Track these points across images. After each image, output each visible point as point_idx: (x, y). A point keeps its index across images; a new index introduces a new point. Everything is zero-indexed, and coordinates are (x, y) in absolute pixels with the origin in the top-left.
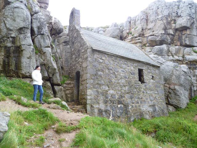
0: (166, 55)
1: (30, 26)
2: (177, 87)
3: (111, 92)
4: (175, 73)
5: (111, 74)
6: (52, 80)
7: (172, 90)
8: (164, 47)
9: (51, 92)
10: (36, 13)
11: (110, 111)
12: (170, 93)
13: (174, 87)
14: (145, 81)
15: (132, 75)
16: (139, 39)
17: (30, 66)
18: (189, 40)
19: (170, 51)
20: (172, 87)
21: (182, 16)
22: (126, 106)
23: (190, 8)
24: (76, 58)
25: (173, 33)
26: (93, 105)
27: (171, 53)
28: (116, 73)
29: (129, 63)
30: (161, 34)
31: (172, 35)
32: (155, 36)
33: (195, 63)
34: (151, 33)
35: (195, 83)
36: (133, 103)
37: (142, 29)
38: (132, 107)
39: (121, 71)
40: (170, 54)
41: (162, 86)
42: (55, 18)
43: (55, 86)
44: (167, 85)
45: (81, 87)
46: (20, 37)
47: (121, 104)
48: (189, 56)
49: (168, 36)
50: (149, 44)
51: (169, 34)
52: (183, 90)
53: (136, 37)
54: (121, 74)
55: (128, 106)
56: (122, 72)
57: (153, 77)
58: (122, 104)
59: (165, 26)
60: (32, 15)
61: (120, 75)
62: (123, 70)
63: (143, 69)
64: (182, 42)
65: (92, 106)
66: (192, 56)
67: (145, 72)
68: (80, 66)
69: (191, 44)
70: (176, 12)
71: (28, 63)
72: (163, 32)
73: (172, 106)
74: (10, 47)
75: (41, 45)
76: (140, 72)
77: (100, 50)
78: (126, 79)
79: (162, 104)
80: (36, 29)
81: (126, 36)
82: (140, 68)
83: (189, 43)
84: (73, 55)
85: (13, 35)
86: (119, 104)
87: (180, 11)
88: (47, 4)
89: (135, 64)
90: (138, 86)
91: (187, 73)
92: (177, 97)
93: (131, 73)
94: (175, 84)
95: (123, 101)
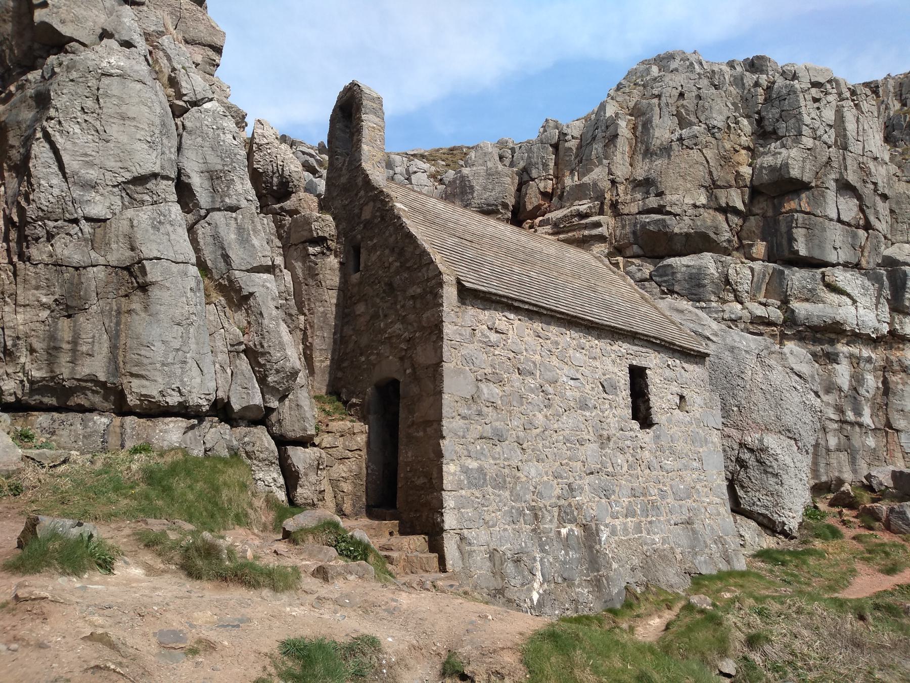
0: (713, 298)
2: (772, 441)
3: (532, 470)
4: (759, 377)
5: (532, 391)
6: (279, 421)
7: (751, 450)
8: (708, 261)
9: (275, 475)
10: (196, 103)
11: (534, 559)
12: (741, 467)
13: (761, 441)
14: (656, 418)
15: (605, 396)
16: (598, 225)
17: (185, 362)
18: (809, 239)
19: (730, 284)
21: (781, 132)
22: (590, 534)
23: (816, 100)
24: (375, 316)
25: (740, 206)
26: (465, 532)
27: (735, 291)
28: (550, 390)
30: (695, 206)
31: (735, 211)
32: (669, 213)
33: (833, 336)
34: (653, 202)
35: (833, 416)
36: (615, 516)
37: (613, 182)
38: (613, 532)
39: (565, 379)
40: (731, 296)
41: (716, 438)
42: (259, 121)
43: (291, 450)
44: (733, 432)
45: (406, 455)
46: (135, 223)
47: (570, 522)
48: (806, 305)
49: (720, 217)
50: (640, 247)
51: (728, 210)
53: (587, 216)
54: (569, 393)
55: (598, 530)
56: (572, 382)
57: (682, 398)
58: (573, 521)
59: (711, 173)
60: (178, 112)
61: (563, 397)
62: (573, 373)
63: (646, 368)
64: (779, 245)
65: (462, 538)
66: (821, 305)
67: (654, 378)
68: (402, 359)
69: (817, 254)
70: (756, 116)
71: (176, 344)
72: (703, 200)
73: (748, 518)
74: (85, 268)
75: (226, 258)
76: (637, 375)
77: (490, 293)
78: (588, 414)
79: (719, 514)
80: (197, 181)
81: (538, 207)
82: (634, 363)
83: (808, 249)
84: (359, 301)
85: (96, 210)
86: (562, 522)
87: (775, 112)
88: (218, 50)
89: (615, 347)
90: (628, 443)
91: (809, 379)
92: (772, 480)
93: (605, 384)
95: (579, 507)
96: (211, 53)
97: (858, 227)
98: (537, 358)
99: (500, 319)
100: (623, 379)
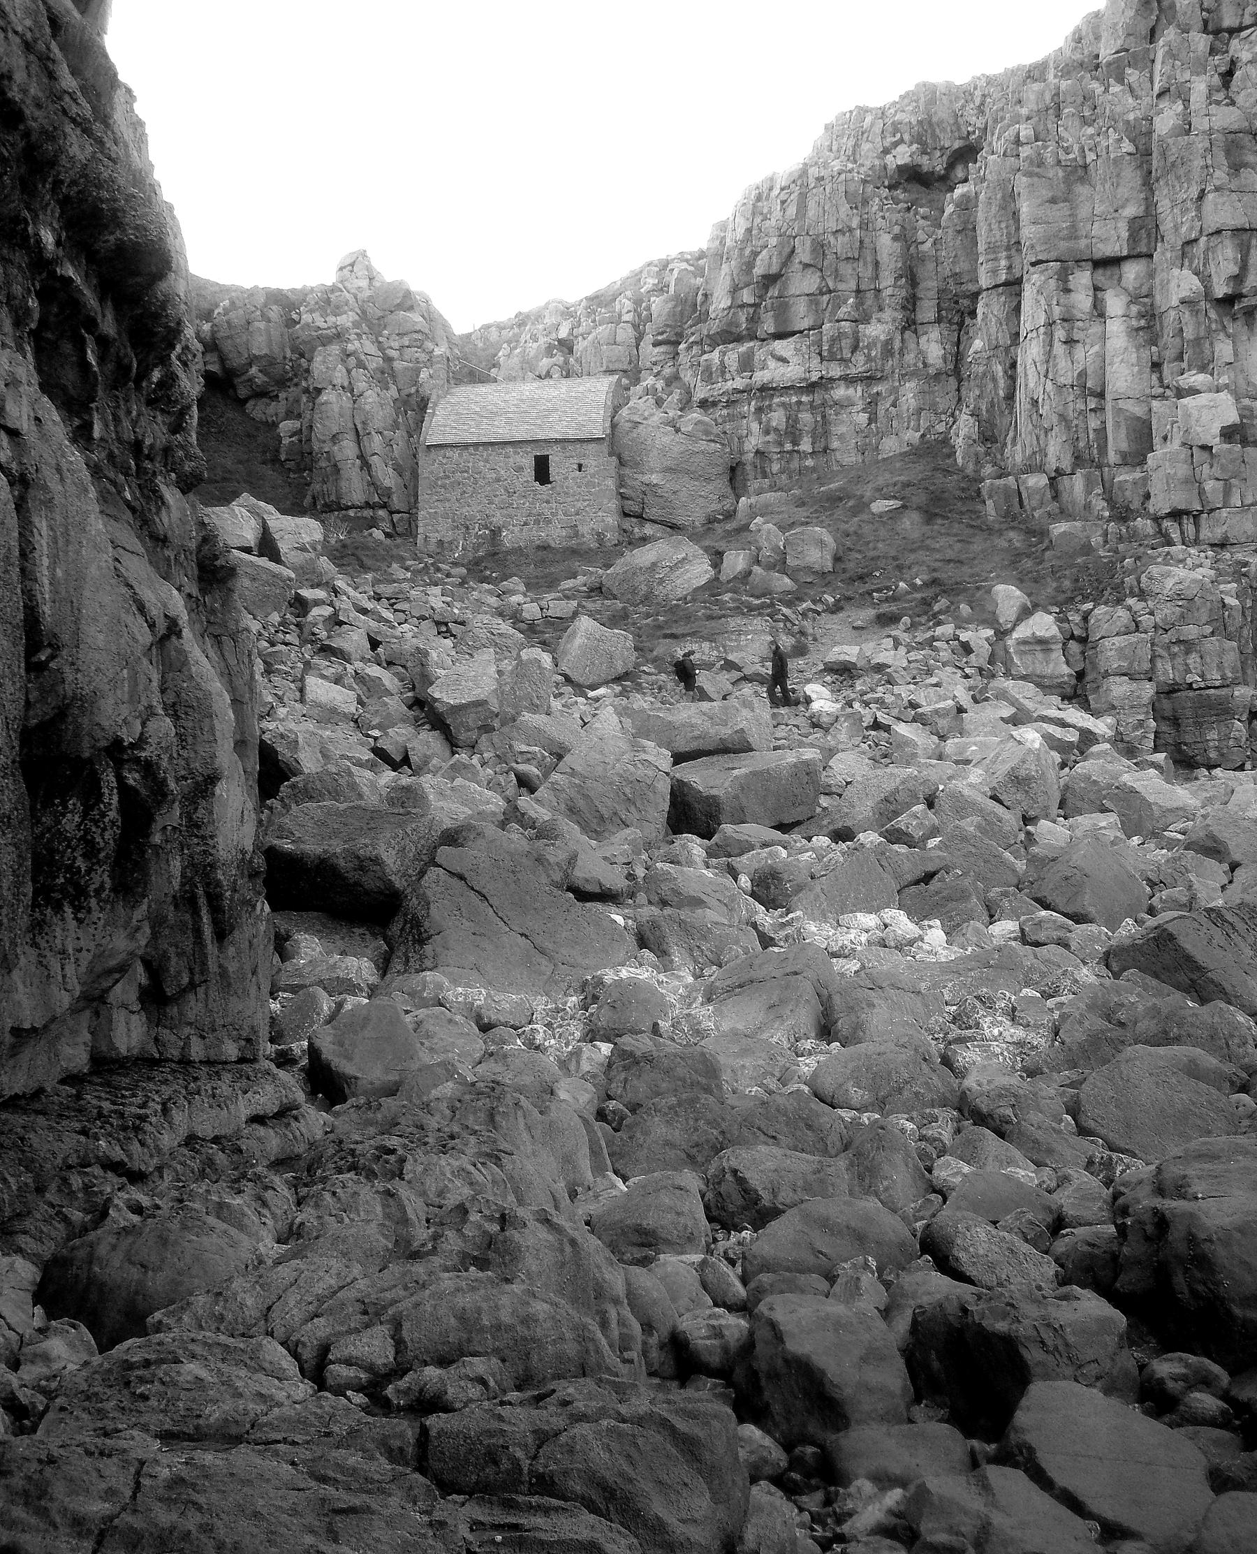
1: (351, 425)
2: (655, 478)
20: (646, 478)
22: (495, 533)
29: (510, 450)
52: (686, 478)
80: (359, 427)
94: (652, 471)
96: (415, 336)
97: (822, 294)
98: (470, 465)
99: (449, 453)
100: (528, 463)
